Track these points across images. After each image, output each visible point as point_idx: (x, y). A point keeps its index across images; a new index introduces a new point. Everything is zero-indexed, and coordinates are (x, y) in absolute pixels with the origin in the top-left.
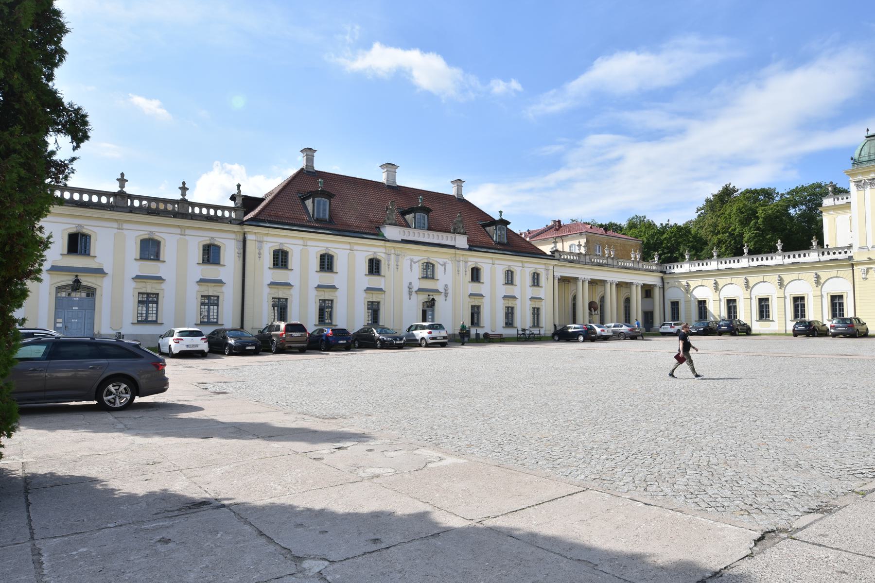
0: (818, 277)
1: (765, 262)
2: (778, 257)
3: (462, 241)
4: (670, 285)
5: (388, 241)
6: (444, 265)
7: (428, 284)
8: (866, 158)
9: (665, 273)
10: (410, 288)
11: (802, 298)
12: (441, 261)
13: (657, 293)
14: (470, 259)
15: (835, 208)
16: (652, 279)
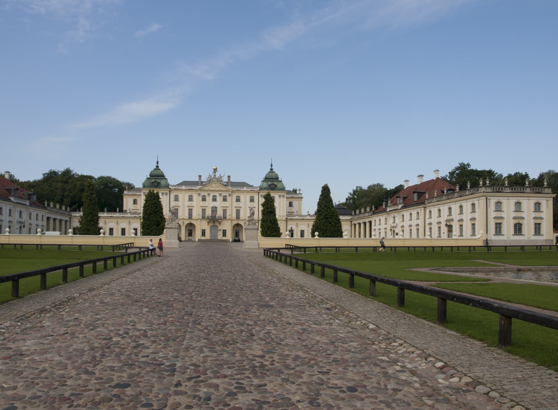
0: (130, 222)
1: (112, 215)
2: (117, 214)
3: (27, 203)
4: (73, 221)
5: (14, 203)
6: (24, 212)
7: (19, 220)
8: (146, 185)
9: (71, 215)
10: (17, 221)
11: (124, 229)
12: (23, 210)
13: (68, 223)
14: (30, 210)
15: (128, 195)
16: (68, 219)
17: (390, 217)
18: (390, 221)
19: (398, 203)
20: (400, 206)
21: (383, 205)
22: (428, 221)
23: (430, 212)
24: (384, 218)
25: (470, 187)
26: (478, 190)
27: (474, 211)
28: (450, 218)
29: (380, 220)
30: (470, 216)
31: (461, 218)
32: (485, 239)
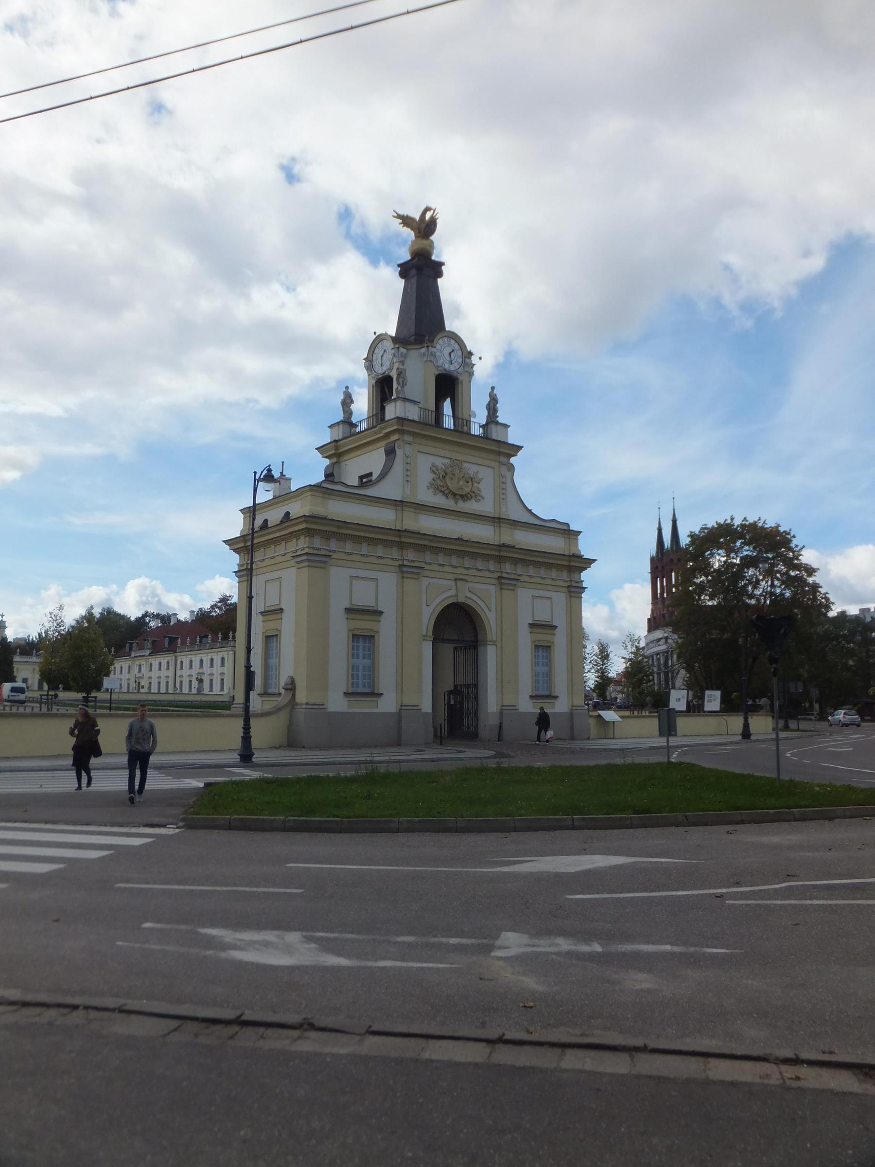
17: (135, 666)
18: (136, 669)
19: (146, 648)
20: (148, 652)
21: (125, 647)
22: (178, 675)
23: (182, 662)
24: (127, 666)
25: (221, 640)
26: (227, 643)
27: (223, 664)
28: (201, 671)
29: (121, 667)
30: (220, 670)
31: (211, 672)
32: (232, 695)
